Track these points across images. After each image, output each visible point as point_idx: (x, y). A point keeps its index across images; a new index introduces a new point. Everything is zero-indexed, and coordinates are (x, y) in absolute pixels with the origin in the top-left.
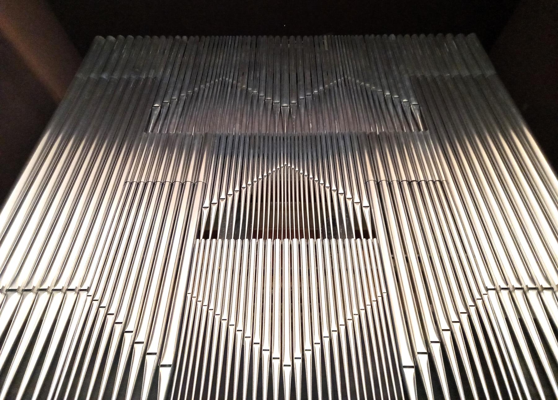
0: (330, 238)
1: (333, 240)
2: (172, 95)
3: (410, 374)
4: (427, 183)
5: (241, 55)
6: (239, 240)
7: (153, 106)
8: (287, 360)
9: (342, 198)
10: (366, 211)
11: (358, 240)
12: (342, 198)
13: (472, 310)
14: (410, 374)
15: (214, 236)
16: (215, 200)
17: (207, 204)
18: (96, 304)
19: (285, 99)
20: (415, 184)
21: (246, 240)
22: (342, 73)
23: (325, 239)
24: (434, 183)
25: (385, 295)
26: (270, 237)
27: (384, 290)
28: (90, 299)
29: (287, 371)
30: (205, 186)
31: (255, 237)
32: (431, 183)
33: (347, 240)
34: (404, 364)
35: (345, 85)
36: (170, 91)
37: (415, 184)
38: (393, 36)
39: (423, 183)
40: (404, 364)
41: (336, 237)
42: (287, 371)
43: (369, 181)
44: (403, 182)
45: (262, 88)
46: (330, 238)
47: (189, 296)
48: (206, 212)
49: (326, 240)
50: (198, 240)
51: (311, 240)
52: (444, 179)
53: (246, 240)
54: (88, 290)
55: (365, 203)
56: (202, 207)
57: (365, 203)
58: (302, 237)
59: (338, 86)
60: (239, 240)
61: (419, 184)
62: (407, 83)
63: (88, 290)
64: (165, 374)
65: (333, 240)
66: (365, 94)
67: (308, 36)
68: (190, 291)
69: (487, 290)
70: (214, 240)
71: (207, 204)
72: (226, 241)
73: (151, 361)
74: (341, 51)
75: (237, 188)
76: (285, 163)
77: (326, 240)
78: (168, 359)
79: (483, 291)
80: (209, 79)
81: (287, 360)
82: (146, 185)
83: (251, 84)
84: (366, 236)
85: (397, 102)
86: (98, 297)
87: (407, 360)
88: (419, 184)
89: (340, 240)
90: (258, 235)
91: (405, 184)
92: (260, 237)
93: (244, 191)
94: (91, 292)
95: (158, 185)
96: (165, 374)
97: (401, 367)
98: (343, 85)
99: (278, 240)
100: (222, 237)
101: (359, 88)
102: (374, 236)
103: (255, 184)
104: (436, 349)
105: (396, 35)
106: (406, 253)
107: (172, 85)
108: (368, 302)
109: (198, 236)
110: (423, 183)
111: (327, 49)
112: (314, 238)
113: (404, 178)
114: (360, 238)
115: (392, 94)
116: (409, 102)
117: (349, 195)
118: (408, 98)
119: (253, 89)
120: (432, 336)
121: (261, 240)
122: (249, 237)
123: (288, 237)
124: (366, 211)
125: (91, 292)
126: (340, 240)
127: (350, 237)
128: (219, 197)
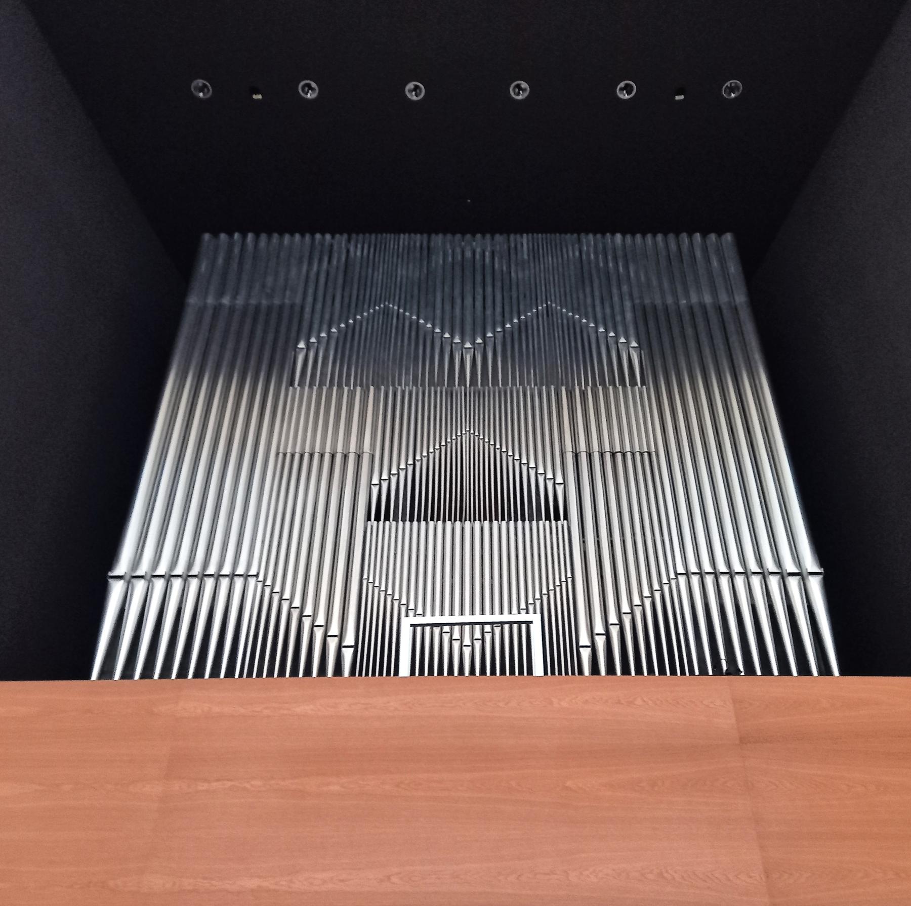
0: (516, 520)
1: (520, 523)
2: (319, 332)
3: (586, 654)
4: (633, 454)
5: (408, 268)
6: (415, 523)
7: (296, 347)
8: (467, 641)
9: (532, 473)
10: (560, 490)
11: (547, 522)
12: (532, 473)
13: (657, 595)
14: (586, 654)
15: (387, 518)
16: (385, 476)
17: (375, 481)
18: (268, 591)
19: (467, 338)
20: (619, 456)
21: (423, 523)
22: (544, 298)
23: (511, 522)
24: (642, 454)
25: (570, 581)
26: (450, 519)
27: (569, 575)
28: (260, 585)
29: (467, 652)
30: (373, 457)
31: (432, 519)
32: (638, 454)
33: (534, 523)
34: (581, 644)
35: (548, 315)
36: (316, 326)
37: (619, 456)
38: (618, 236)
39: (629, 455)
40: (581, 644)
41: (523, 520)
42: (467, 652)
43: (565, 452)
44: (606, 453)
45: (438, 321)
46: (516, 520)
47: (365, 582)
48: (375, 490)
49: (512, 523)
50: (369, 522)
51: (495, 523)
52: (653, 449)
53: (423, 523)
54: (257, 576)
55: (559, 480)
56: (370, 484)
57: (559, 480)
58: (485, 519)
59: (538, 317)
60: (415, 523)
61: (624, 455)
62: (629, 316)
63: (257, 576)
64: (348, 654)
65: (520, 523)
66: (572, 331)
67: (501, 233)
68: (365, 576)
69: (677, 574)
70: (387, 522)
71: (375, 481)
72: (401, 523)
73: (332, 644)
74: (546, 260)
75: (410, 462)
76: (468, 429)
77: (512, 523)
78: (349, 640)
79: (672, 576)
80: (366, 306)
81: (467, 641)
82: (302, 456)
83: (422, 315)
84: (557, 518)
85: (611, 341)
86: (269, 582)
87: (584, 640)
88: (624, 455)
89: (527, 522)
90: (435, 516)
91: (608, 457)
92: (438, 519)
93: (418, 464)
94: (261, 578)
95: (316, 457)
96: (348, 654)
98: (545, 316)
99: (458, 523)
100: (396, 519)
101: (565, 321)
102: (566, 517)
103: (431, 456)
104: (615, 632)
105: (624, 234)
106: (598, 536)
107: (317, 316)
108: (551, 587)
109: (369, 519)
110: (629, 455)
111: (526, 257)
112: (498, 521)
113: (607, 448)
114: (550, 521)
115: (607, 331)
116: (628, 343)
117: (541, 471)
118: (627, 338)
119: (426, 322)
120: (613, 619)
121: (440, 523)
122: (425, 519)
123: (470, 520)
124: (560, 490)
125: (261, 578)
126: (527, 522)
127: (539, 518)
128: (390, 472)
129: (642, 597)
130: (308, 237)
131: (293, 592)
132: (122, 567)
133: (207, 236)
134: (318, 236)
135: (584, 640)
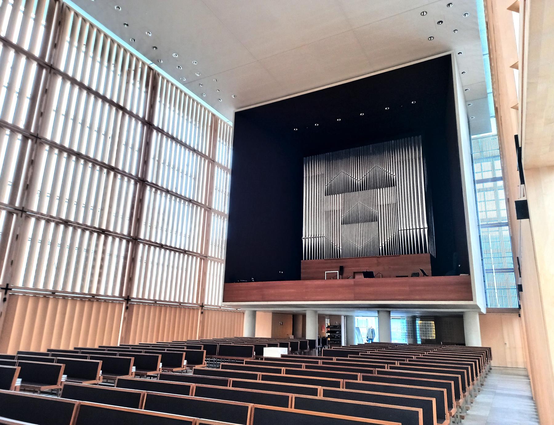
3: (381, 248)
8: (360, 247)
10: (377, 214)
14: (381, 248)
17: (342, 216)
29: (360, 249)
42: (360, 249)
55: (377, 212)
56: (342, 217)
57: (377, 212)
64: (341, 250)
69: (398, 230)
71: (342, 216)
81: (360, 247)
87: (380, 245)
97: (379, 246)
124: (377, 214)
129: (391, 236)
130: (324, 154)
131: (331, 239)
132: (304, 237)
133: (304, 158)
134: (326, 154)
135: (380, 245)
